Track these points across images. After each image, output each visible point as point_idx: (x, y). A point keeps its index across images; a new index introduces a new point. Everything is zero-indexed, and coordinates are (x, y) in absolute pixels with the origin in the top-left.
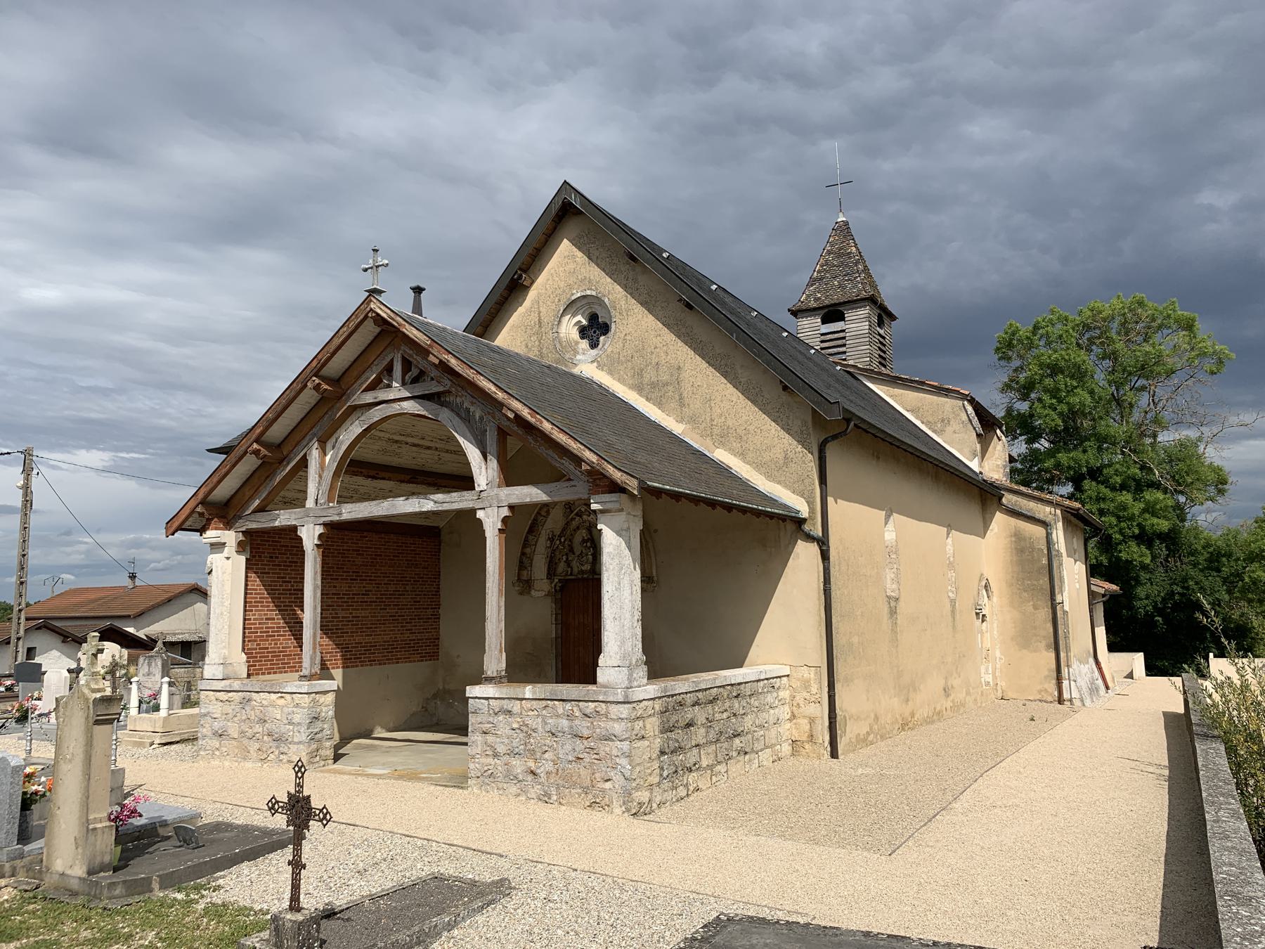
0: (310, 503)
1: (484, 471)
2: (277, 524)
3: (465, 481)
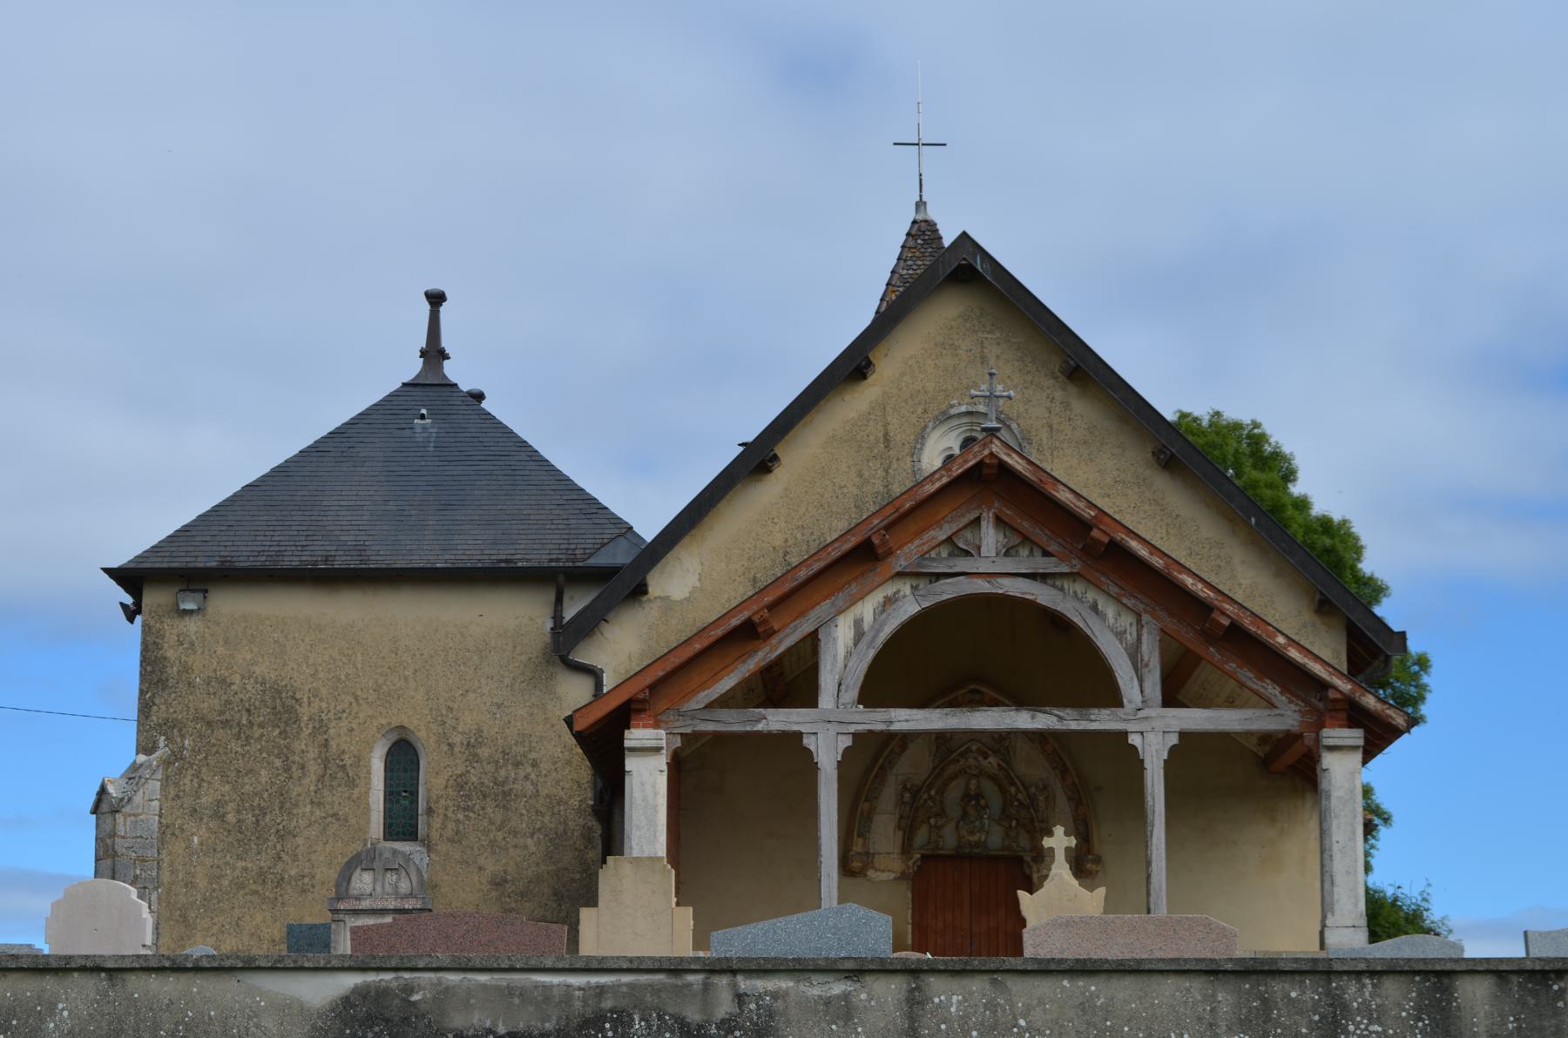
0: (826, 700)
1: (1137, 685)
2: (760, 727)
3: (1111, 697)
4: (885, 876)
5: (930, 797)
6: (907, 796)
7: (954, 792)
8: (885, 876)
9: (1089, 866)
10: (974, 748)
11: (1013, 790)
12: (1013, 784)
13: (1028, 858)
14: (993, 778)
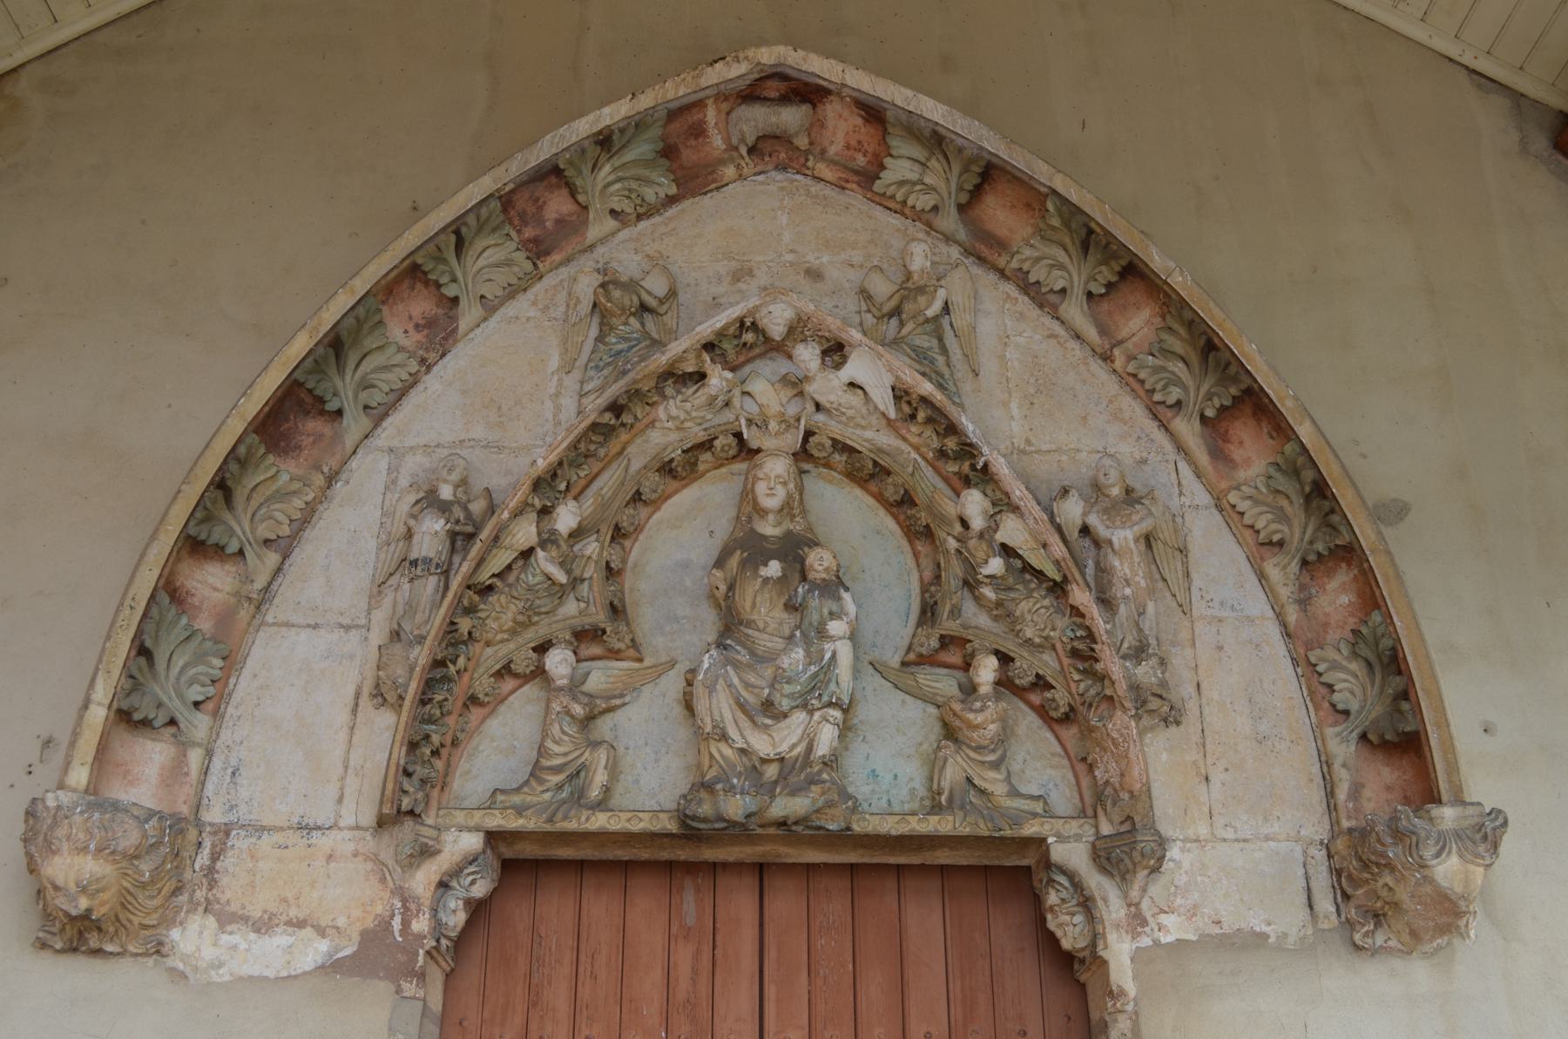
4: (273, 953)
5: (548, 540)
6: (431, 533)
7: (681, 538)
8: (273, 953)
9: (1448, 869)
10: (777, 319)
11: (974, 504)
12: (983, 476)
13: (1072, 852)
14: (868, 473)
